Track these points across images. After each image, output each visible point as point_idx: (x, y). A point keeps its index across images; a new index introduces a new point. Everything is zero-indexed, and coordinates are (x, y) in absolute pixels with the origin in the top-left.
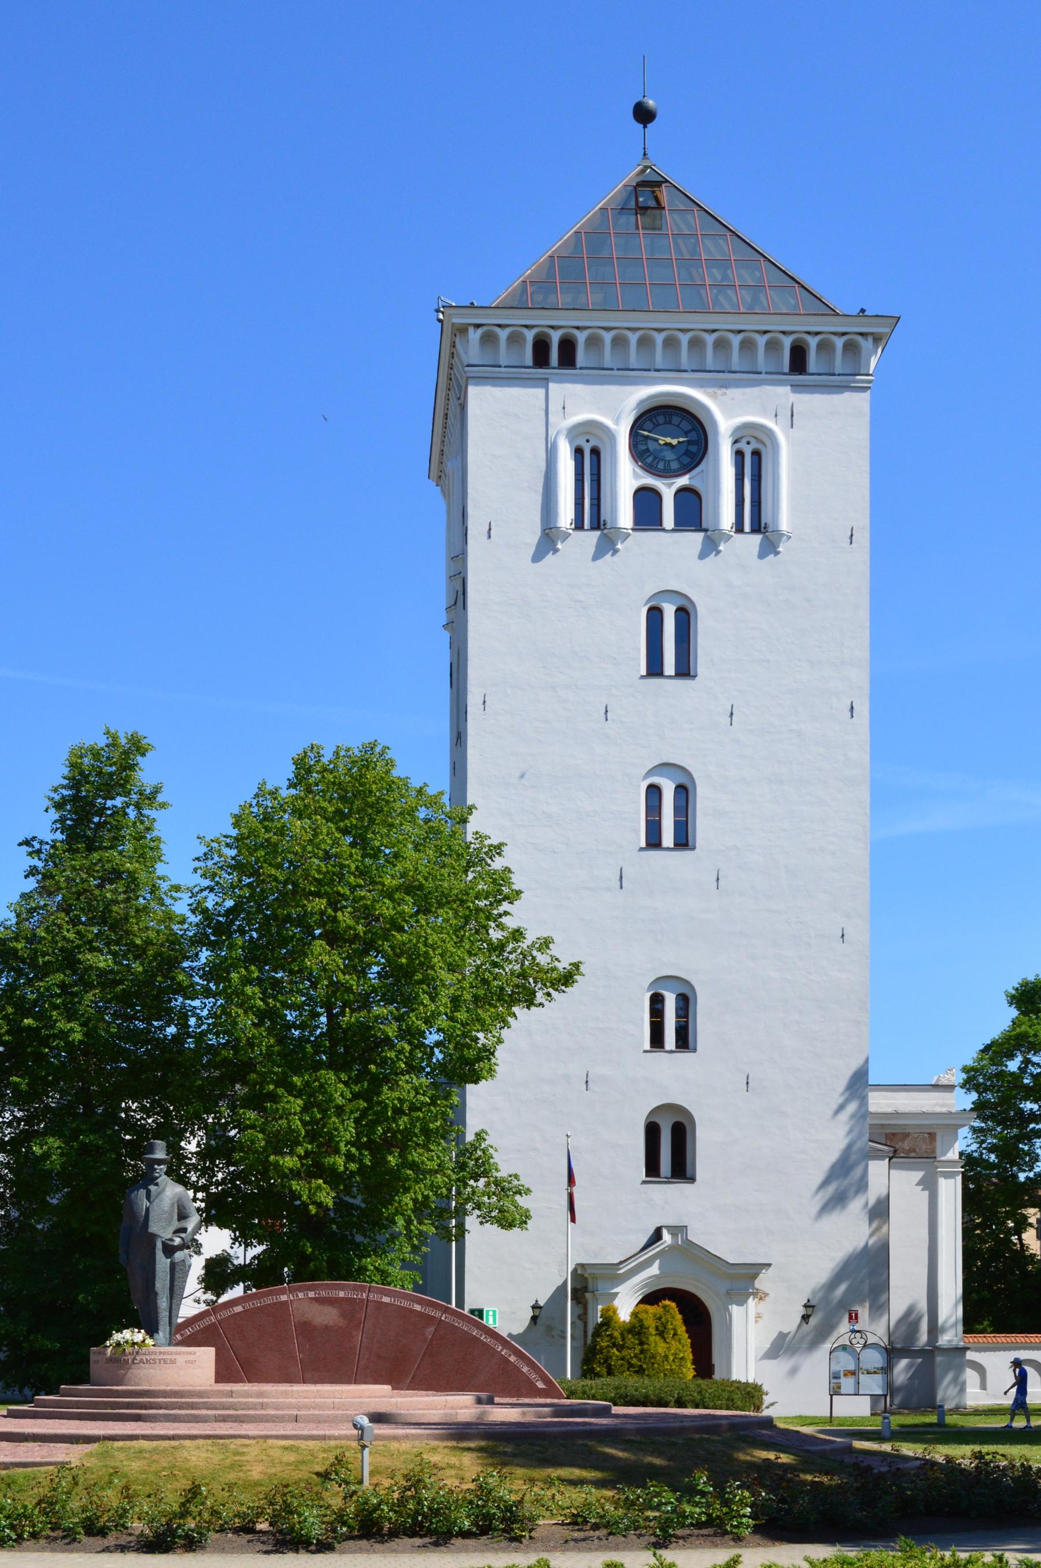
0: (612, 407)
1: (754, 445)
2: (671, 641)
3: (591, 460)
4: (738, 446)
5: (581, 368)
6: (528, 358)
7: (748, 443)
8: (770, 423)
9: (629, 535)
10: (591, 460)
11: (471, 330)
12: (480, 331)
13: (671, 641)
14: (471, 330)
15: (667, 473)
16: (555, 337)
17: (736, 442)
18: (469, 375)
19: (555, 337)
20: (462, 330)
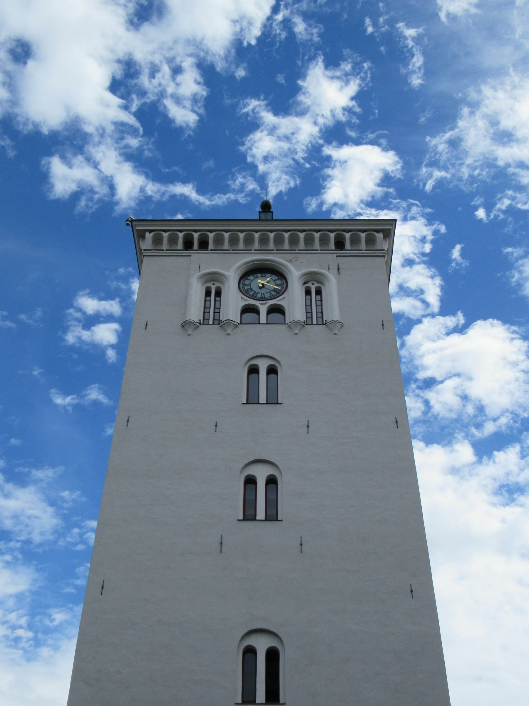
0: (230, 267)
1: (316, 285)
2: (262, 380)
3: (214, 293)
4: (306, 285)
5: (211, 250)
6: (180, 245)
7: (313, 284)
8: (325, 272)
9: (237, 326)
10: (214, 293)
11: (147, 234)
12: (152, 234)
13: (262, 380)
14: (147, 234)
15: (263, 299)
16: (196, 235)
17: (305, 283)
18: (144, 254)
19: (196, 235)
20: (141, 235)
